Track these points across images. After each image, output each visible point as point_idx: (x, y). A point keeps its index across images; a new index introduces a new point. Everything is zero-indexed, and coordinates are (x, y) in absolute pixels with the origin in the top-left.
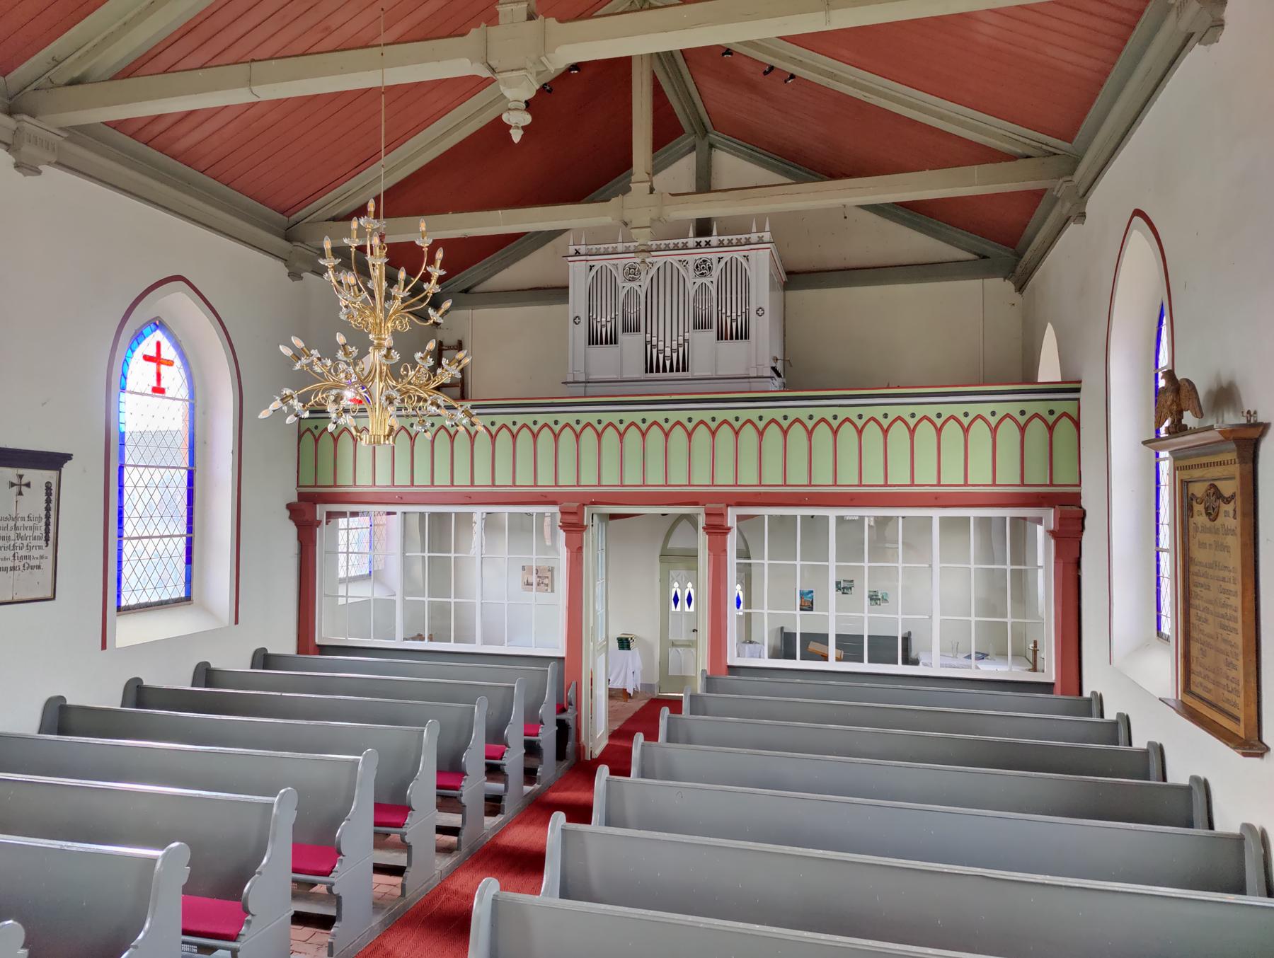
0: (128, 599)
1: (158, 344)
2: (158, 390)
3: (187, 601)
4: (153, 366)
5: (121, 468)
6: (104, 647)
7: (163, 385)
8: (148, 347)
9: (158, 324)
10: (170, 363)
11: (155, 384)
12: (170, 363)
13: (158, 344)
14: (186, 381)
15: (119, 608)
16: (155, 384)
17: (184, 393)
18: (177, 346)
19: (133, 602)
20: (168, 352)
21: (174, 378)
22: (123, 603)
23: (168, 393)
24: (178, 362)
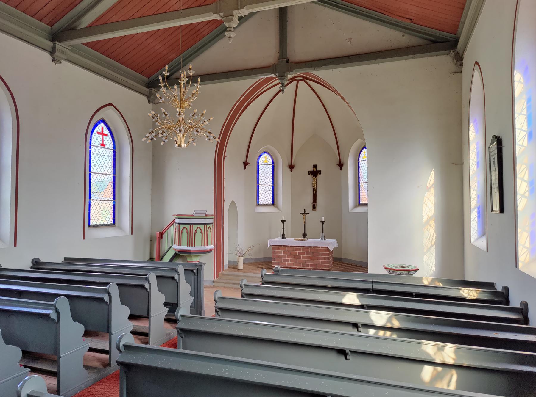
0: (93, 222)
1: (102, 128)
2: (103, 145)
3: (113, 225)
4: (101, 136)
5: (90, 174)
6: (84, 238)
7: (104, 143)
8: (98, 129)
9: (103, 121)
10: (106, 135)
11: (101, 142)
12: (106, 135)
13: (102, 128)
14: (112, 142)
15: (89, 225)
16: (101, 142)
17: (112, 147)
18: (109, 129)
19: (94, 223)
20: (106, 131)
21: (108, 140)
22: (91, 224)
23: (106, 147)
24: (109, 135)
